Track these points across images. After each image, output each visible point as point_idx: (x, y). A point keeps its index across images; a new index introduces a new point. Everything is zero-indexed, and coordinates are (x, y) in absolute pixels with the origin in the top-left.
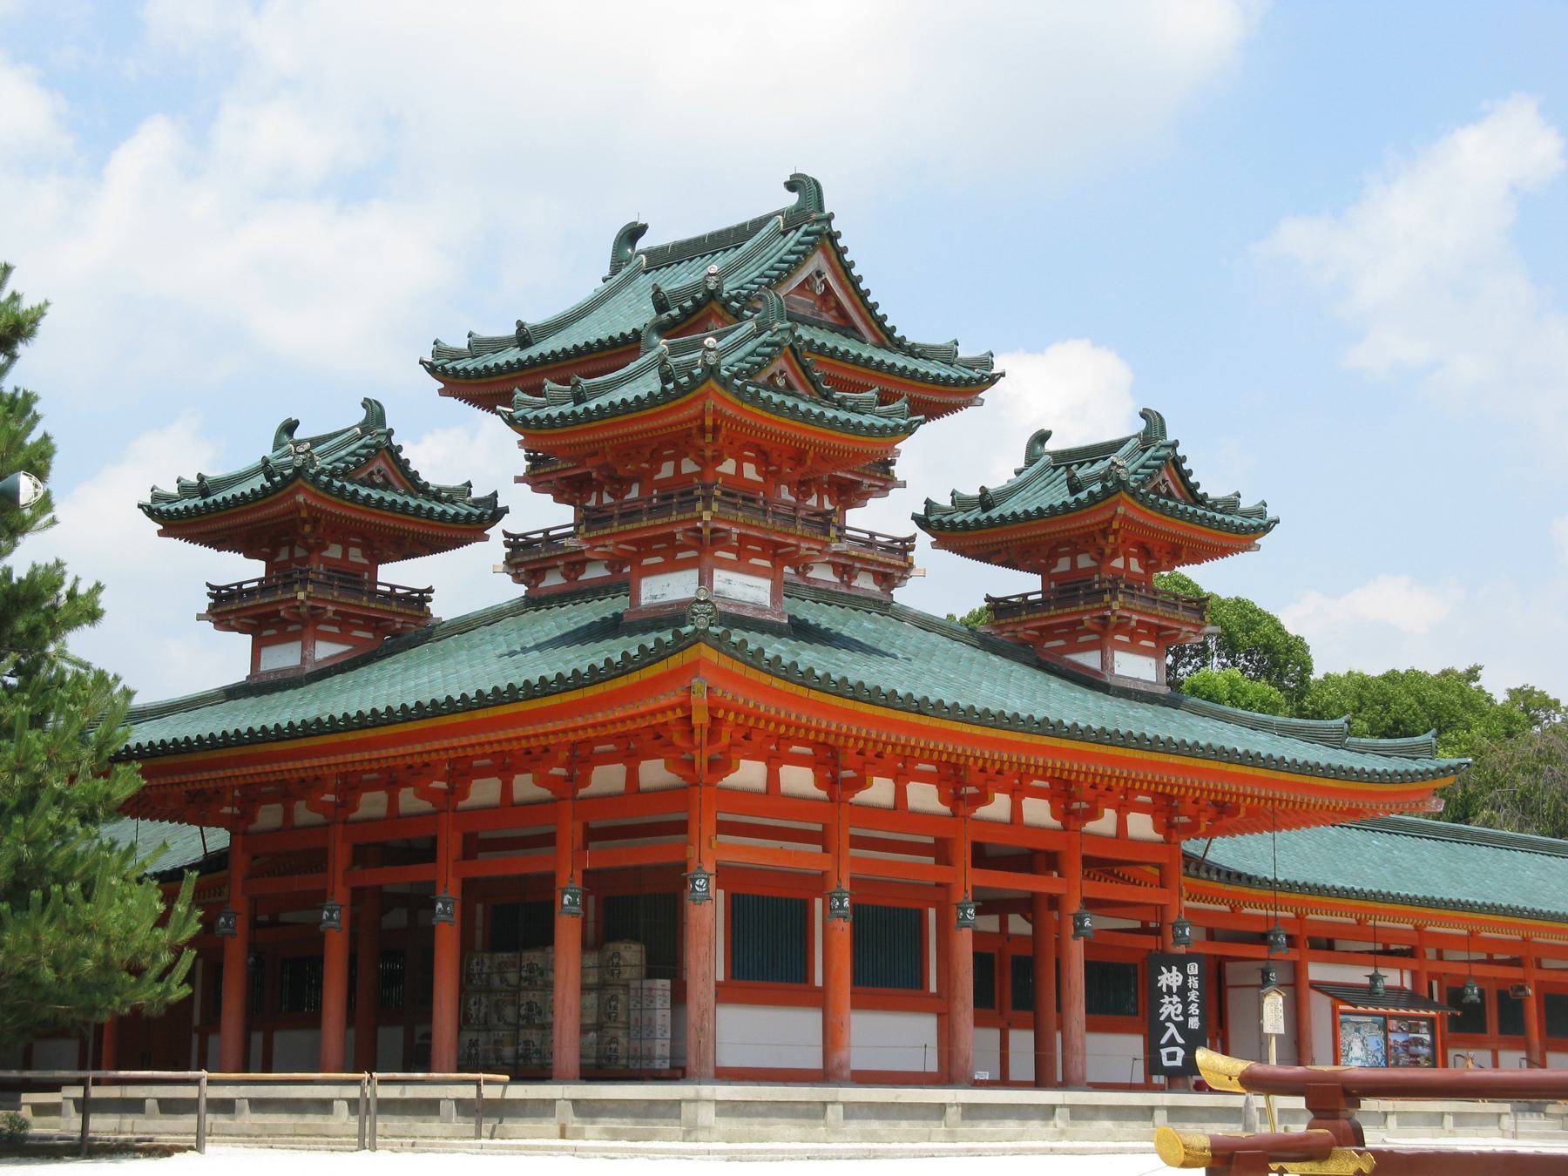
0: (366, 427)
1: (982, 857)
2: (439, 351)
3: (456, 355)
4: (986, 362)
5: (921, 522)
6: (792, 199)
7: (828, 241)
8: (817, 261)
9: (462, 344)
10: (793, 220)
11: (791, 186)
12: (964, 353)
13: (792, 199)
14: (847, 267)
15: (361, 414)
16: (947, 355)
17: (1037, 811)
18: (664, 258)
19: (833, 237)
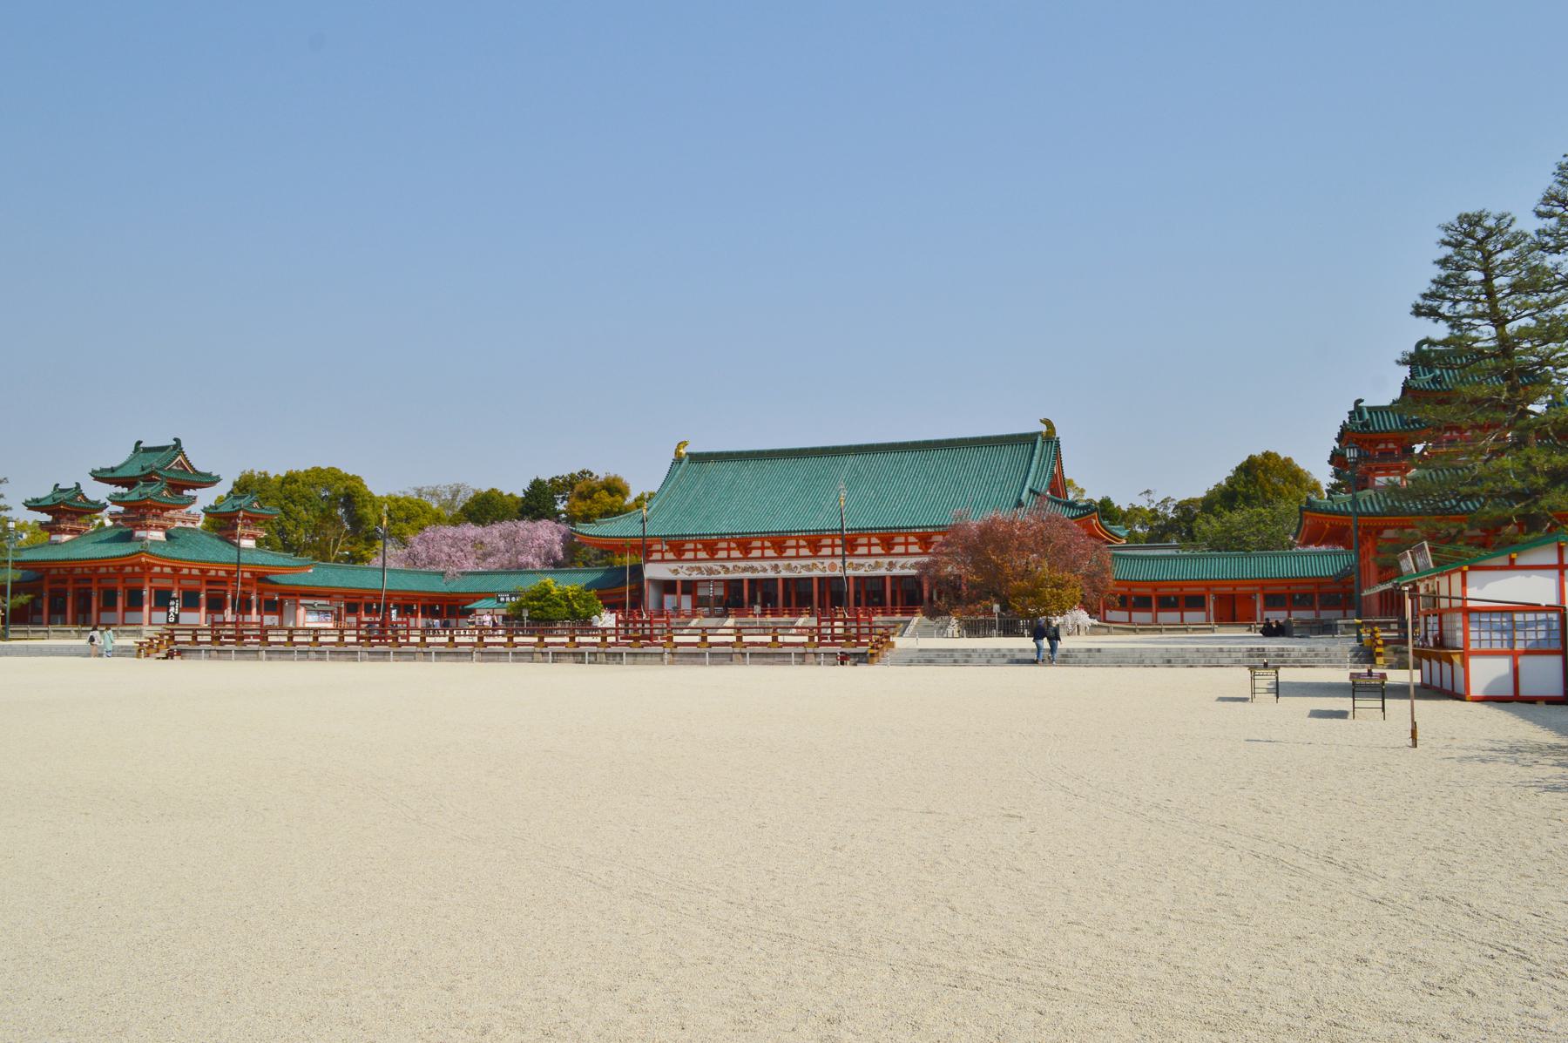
0: (76, 488)
1: (209, 582)
2: (93, 471)
3: (97, 472)
4: (218, 477)
5: (203, 511)
6: (175, 443)
7: (181, 452)
8: (180, 458)
9: (98, 469)
10: (175, 447)
11: (175, 439)
12: (214, 474)
13: (175, 443)
14: (186, 458)
15: (75, 486)
16: (209, 475)
17: (222, 573)
18: (147, 450)
19: (183, 452)
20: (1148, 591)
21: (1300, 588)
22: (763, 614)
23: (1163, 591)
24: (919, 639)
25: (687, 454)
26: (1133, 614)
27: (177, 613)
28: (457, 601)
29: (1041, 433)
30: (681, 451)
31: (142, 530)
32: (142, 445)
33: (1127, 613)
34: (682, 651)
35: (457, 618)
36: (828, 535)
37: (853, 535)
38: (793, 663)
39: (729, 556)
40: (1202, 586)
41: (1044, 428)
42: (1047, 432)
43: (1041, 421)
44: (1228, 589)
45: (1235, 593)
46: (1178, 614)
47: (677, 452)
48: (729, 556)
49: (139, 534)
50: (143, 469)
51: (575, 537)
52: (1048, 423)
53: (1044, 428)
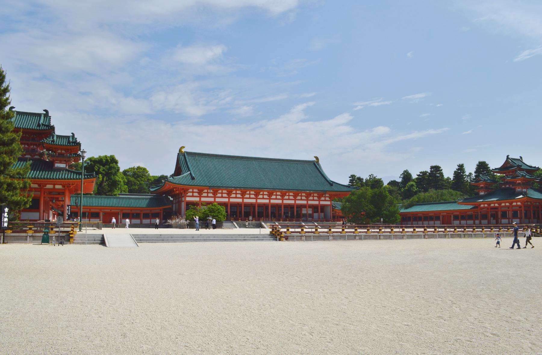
13: (45, 112)
20: (139, 211)
22: (252, 220)
23: (133, 211)
24: (261, 229)
25: (185, 152)
26: (467, 221)
27: (69, 214)
28: (440, 214)
29: (315, 161)
30: (182, 150)
31: (61, 163)
32: (13, 110)
33: (466, 221)
34: (469, 234)
35: (429, 221)
36: (266, 191)
37: (285, 191)
38: (378, 239)
39: (222, 196)
40: (119, 209)
41: (315, 159)
42: (317, 161)
43: (315, 157)
44: (157, 211)
45: (90, 211)
46: (417, 222)
47: (180, 150)
48: (222, 196)
49: (57, 165)
50: (39, 125)
51: (167, 184)
52: (317, 158)
53: (315, 159)
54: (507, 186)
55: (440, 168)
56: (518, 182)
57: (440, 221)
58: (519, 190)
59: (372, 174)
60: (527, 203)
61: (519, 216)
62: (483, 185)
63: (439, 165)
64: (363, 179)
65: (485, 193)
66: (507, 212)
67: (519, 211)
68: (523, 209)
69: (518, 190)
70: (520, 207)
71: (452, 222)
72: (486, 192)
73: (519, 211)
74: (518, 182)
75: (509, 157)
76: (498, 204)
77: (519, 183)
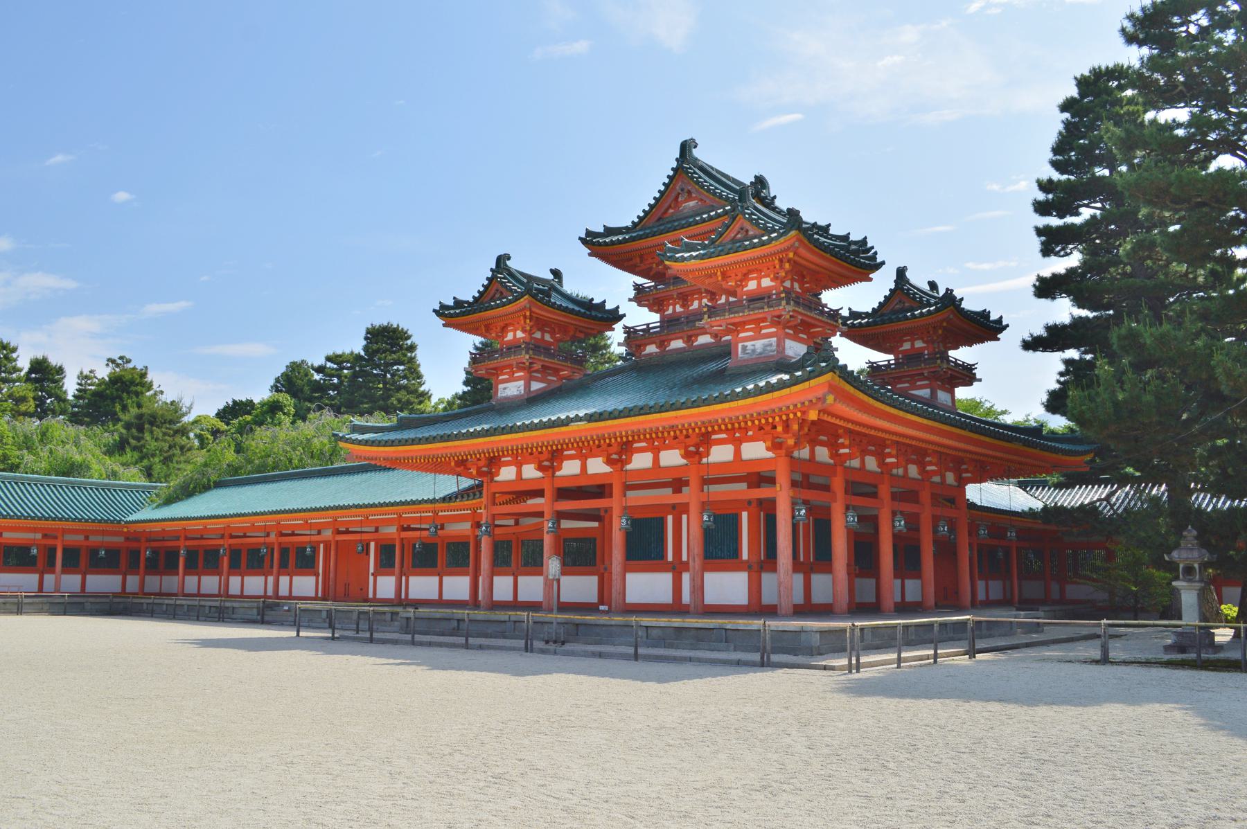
21: (108, 539)
54: (677, 344)
55: (409, 337)
56: (752, 285)
57: (317, 575)
58: (759, 344)
59: (121, 358)
60: (812, 452)
61: (745, 556)
62: (520, 334)
63: (404, 325)
64: (60, 370)
65: (527, 386)
66: (670, 519)
67: (745, 515)
68: (782, 495)
69: (749, 344)
70: (759, 477)
71: (371, 578)
72: (537, 379)
73: (745, 515)
74: (752, 285)
75: (696, 153)
76: (609, 462)
77: (758, 298)
